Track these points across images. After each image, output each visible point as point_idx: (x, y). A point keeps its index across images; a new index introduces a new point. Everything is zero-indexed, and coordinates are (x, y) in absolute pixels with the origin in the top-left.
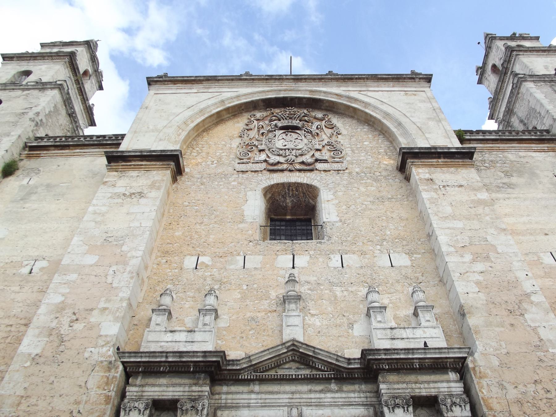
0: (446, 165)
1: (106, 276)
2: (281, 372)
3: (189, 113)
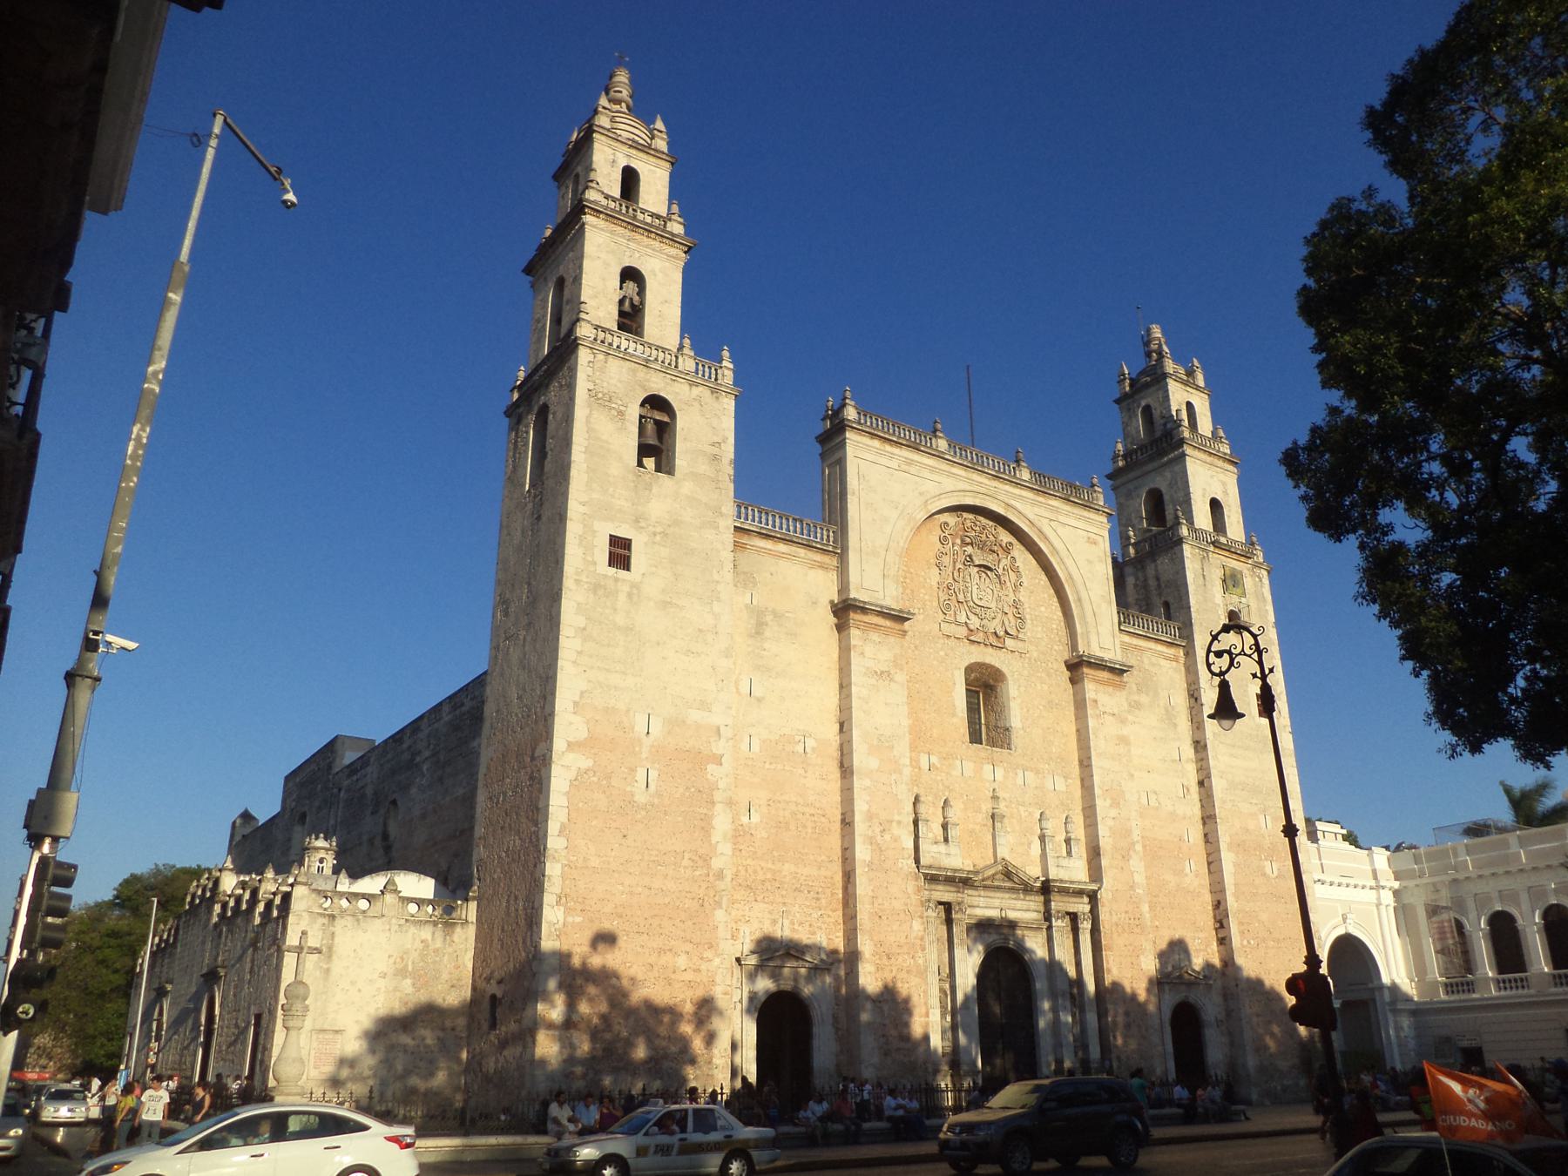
2: (996, 883)
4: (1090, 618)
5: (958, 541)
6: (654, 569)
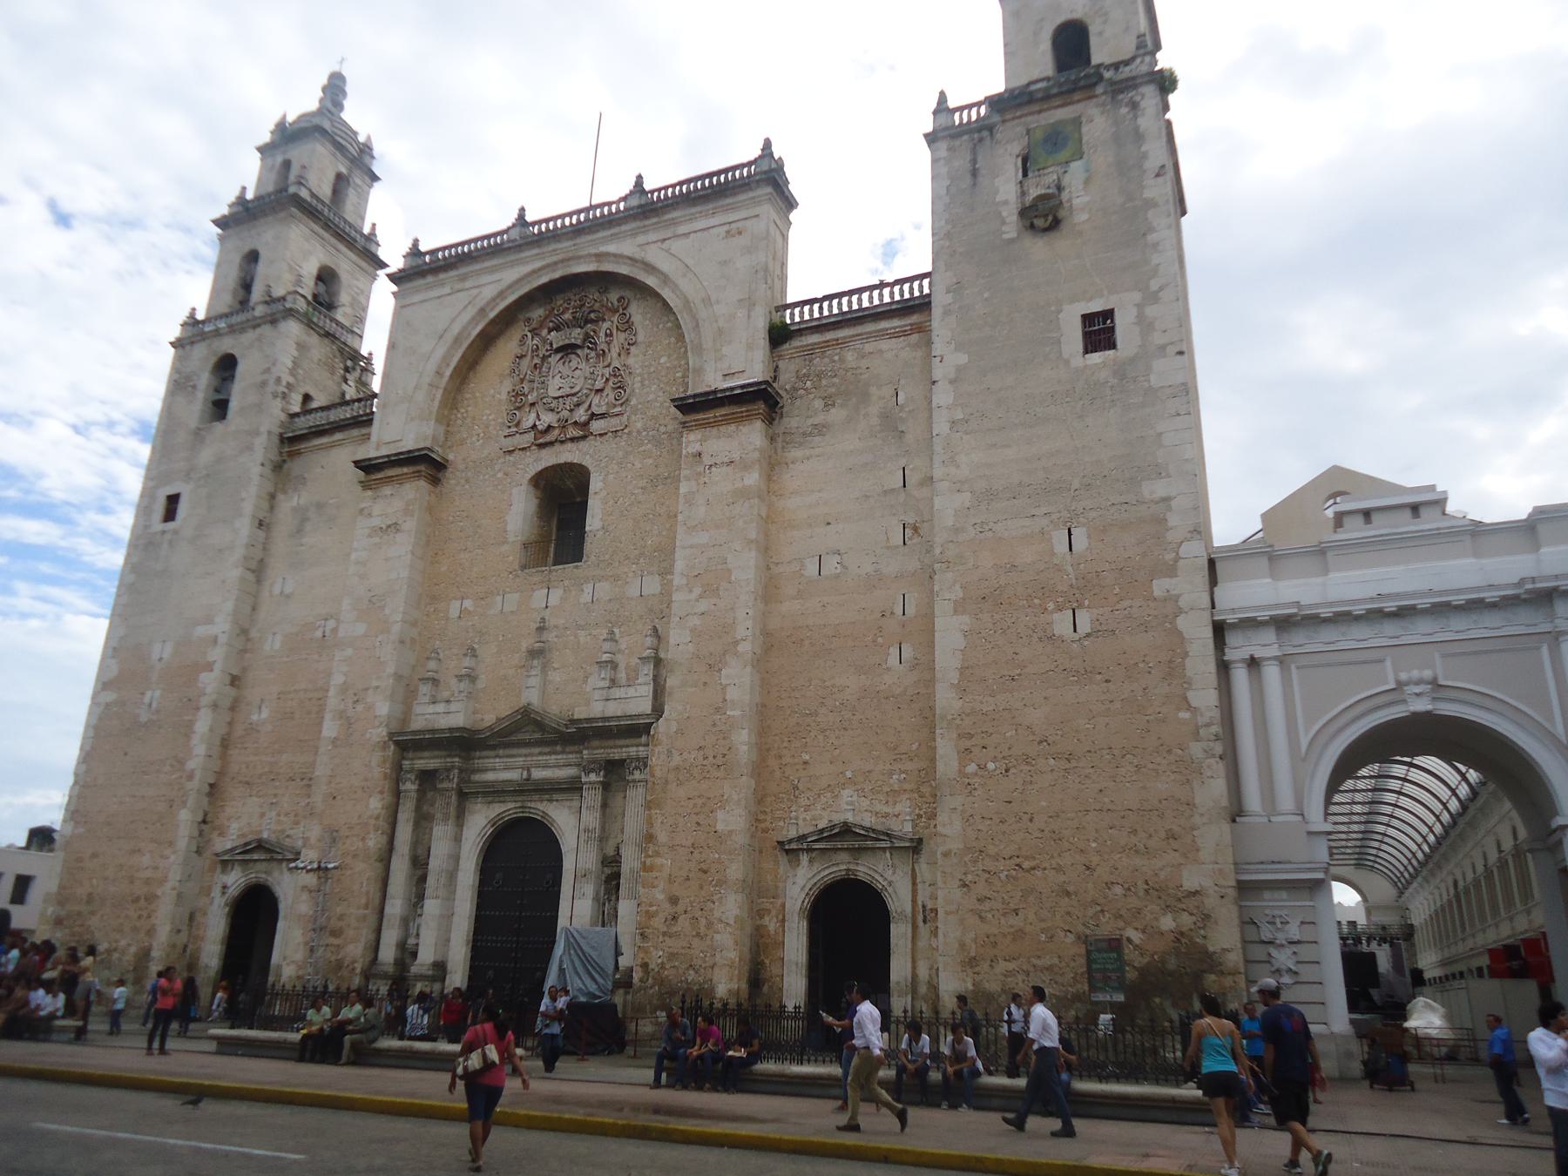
0: (727, 420)
2: (520, 736)
3: (440, 352)
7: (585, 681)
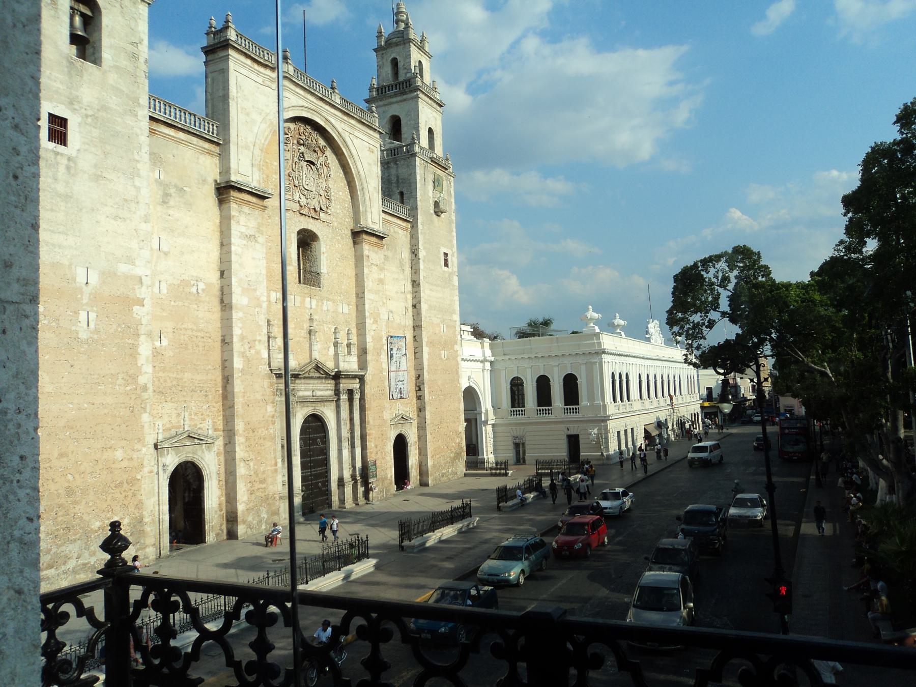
0: (376, 245)
1: (255, 315)
2: (311, 375)
4: (368, 203)
5: (295, 142)
6: (87, 146)
7: (329, 350)
